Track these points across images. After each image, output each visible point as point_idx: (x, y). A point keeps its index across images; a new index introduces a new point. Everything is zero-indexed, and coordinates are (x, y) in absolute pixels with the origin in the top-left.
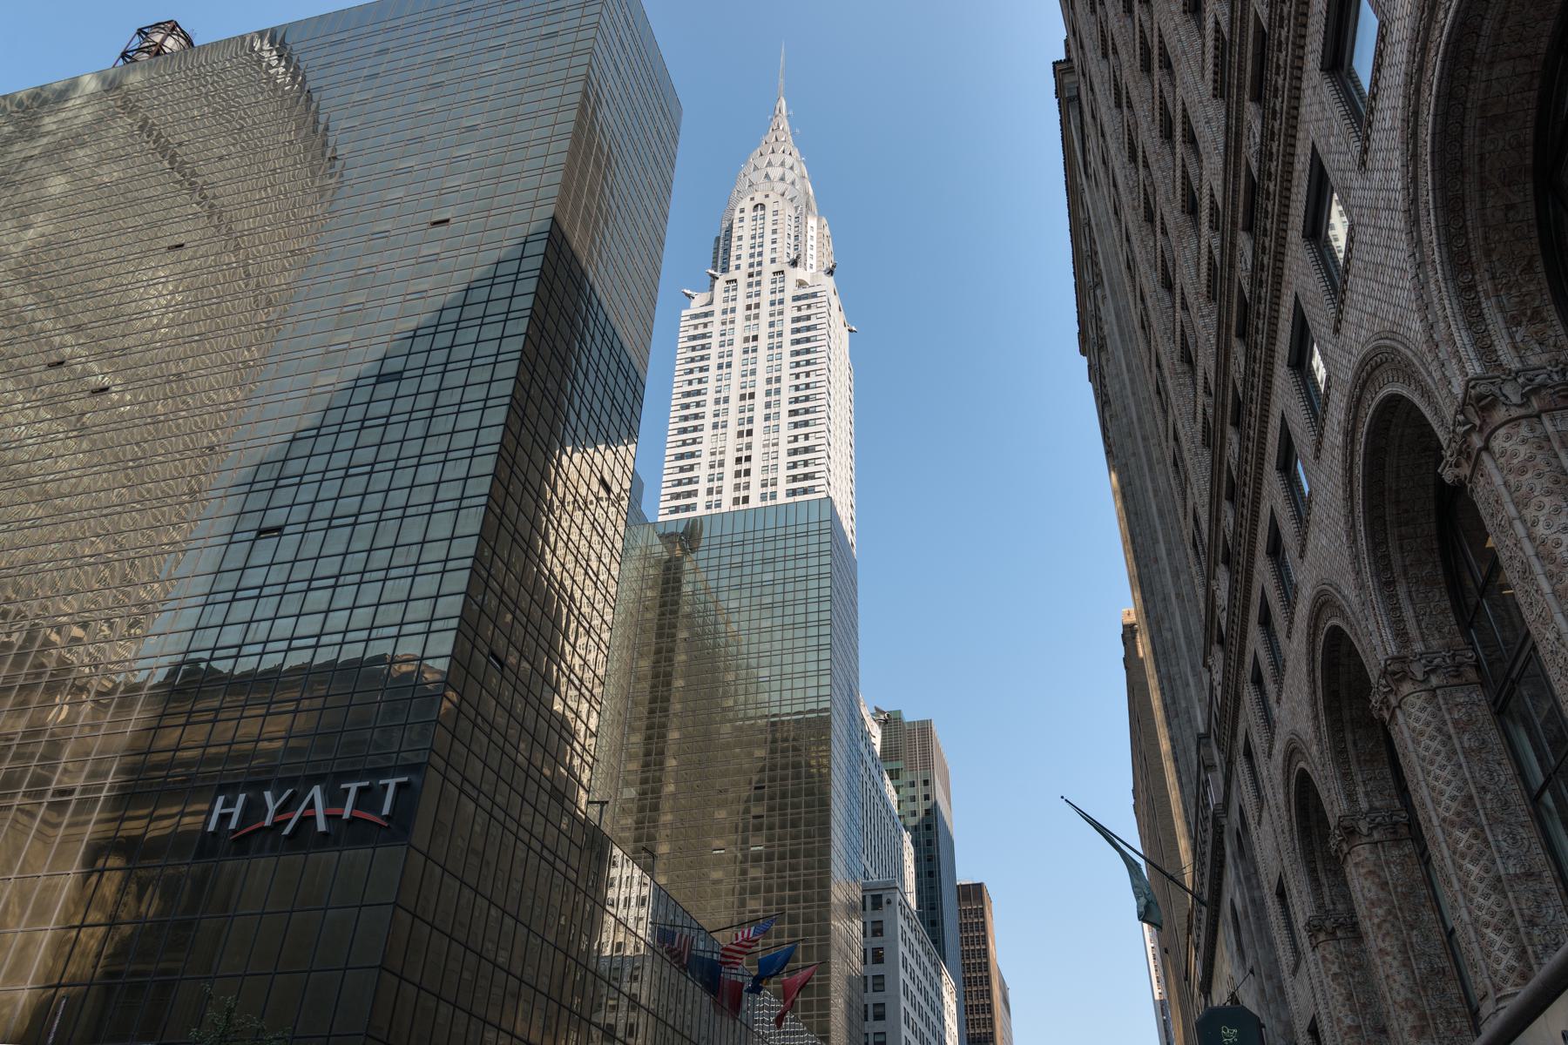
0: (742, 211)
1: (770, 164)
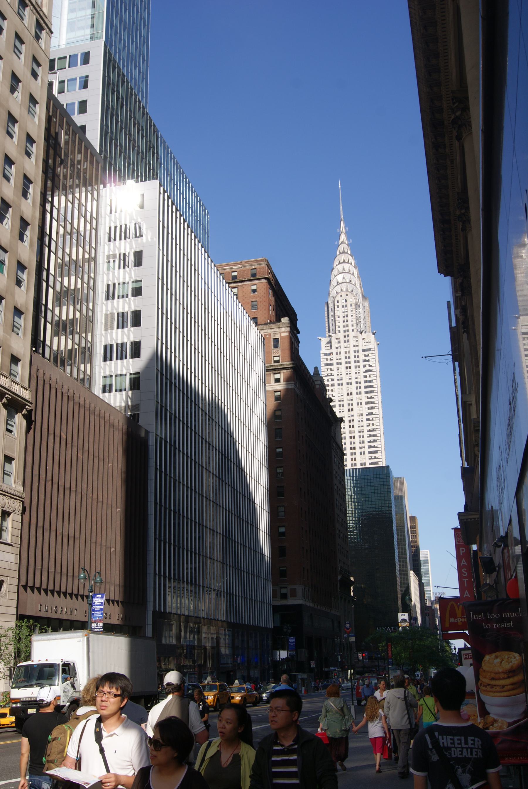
0: (338, 302)
1: (344, 269)
